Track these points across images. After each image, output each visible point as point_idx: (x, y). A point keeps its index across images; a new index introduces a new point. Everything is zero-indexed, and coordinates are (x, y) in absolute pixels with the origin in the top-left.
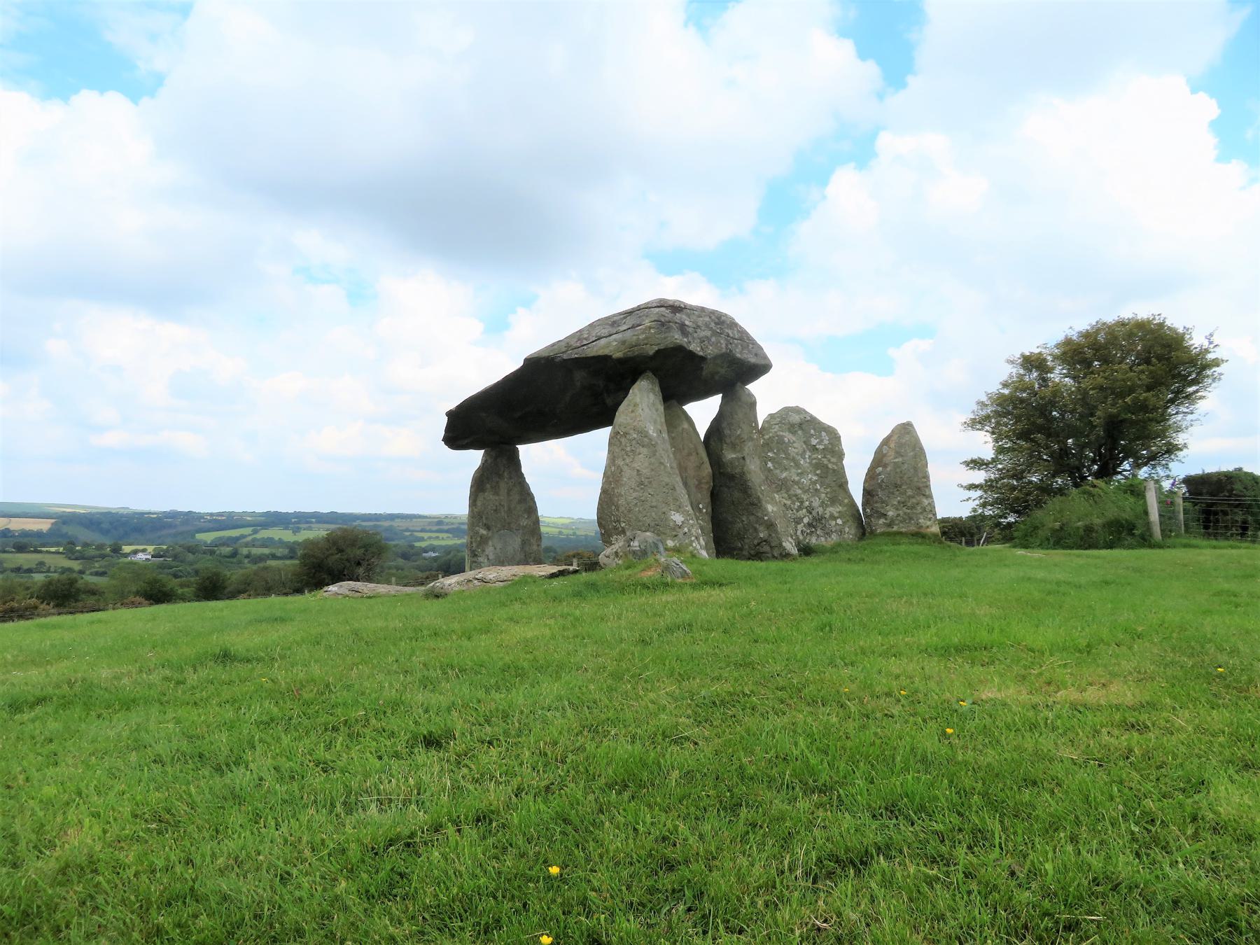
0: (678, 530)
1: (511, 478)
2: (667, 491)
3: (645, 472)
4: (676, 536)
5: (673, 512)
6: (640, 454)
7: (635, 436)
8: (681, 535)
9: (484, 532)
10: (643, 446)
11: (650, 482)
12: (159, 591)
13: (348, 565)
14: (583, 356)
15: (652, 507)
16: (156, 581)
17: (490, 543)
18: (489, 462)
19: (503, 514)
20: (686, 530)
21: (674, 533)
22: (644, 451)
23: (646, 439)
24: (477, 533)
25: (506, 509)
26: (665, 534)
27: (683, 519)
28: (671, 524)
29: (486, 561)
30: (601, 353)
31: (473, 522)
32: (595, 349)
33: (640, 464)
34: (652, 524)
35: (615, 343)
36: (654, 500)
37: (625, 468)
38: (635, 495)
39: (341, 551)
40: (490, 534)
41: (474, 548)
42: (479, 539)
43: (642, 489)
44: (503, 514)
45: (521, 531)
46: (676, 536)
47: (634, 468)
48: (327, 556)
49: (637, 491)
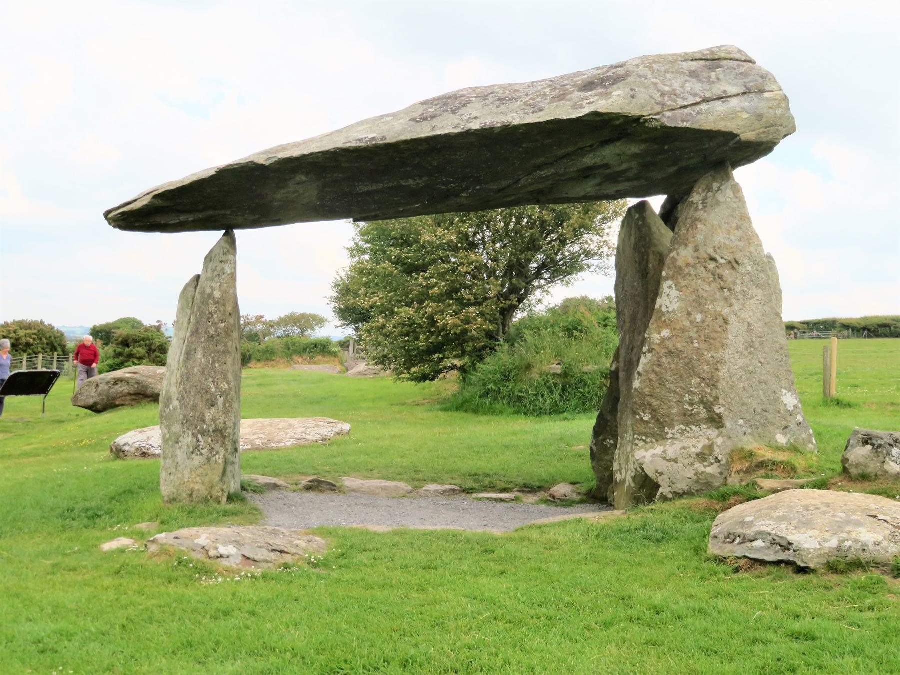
0: (789, 418)
2: (780, 358)
3: (758, 327)
4: (786, 428)
5: (785, 391)
6: (752, 298)
7: (749, 268)
8: (793, 426)
10: (757, 287)
11: (762, 344)
14: (696, 126)
15: (760, 382)
20: (800, 418)
21: (784, 423)
22: (758, 293)
23: (762, 275)
26: (773, 424)
27: (796, 402)
28: (782, 408)
30: (723, 126)
32: (711, 119)
33: (751, 314)
34: (759, 410)
35: (745, 116)
36: (764, 372)
37: (732, 319)
38: (741, 362)
43: (750, 354)
46: (786, 428)
47: (744, 320)
49: (745, 357)
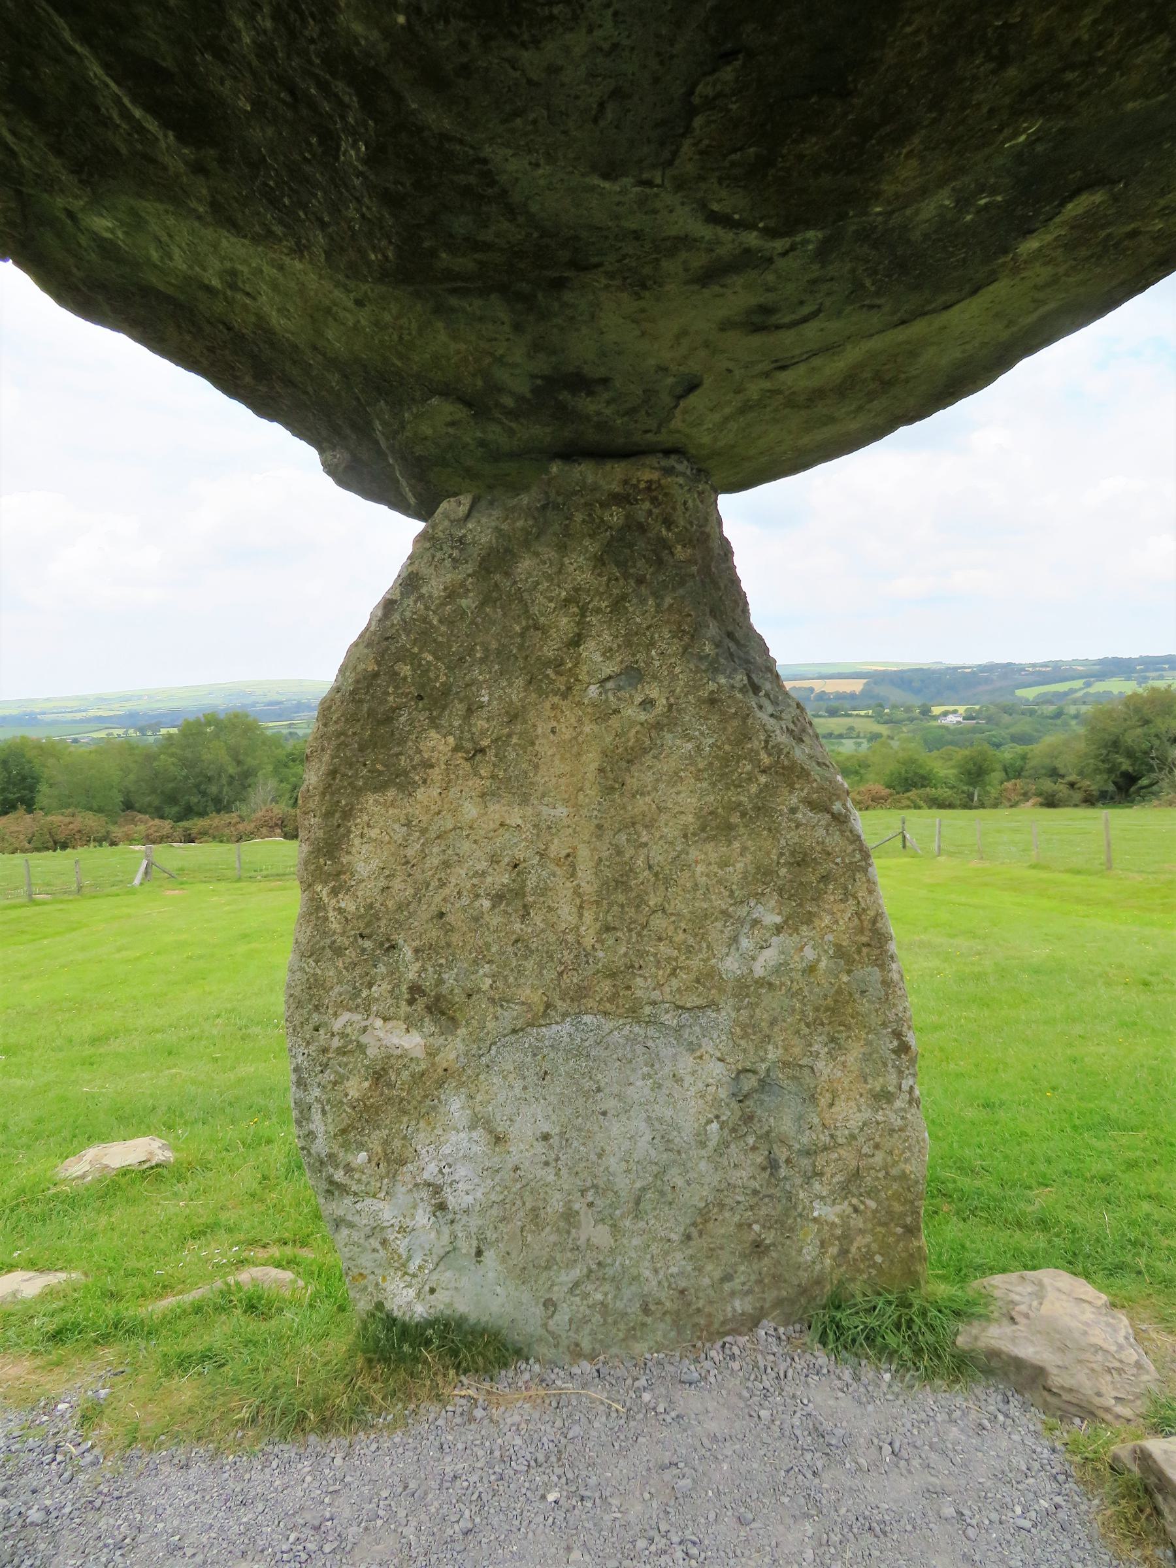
1: (633, 675)
9: (412, 1042)
12: (916, 774)
13: (1157, 742)
16: (913, 761)
17: (455, 1106)
18: (435, 587)
19: (566, 913)
24: (352, 1048)
25: (587, 880)
29: (422, 1218)
31: (315, 984)
39: (1146, 722)
40: (453, 1049)
41: (321, 1146)
42: (356, 1087)
44: (566, 913)
45: (726, 1015)
48: (1125, 730)
